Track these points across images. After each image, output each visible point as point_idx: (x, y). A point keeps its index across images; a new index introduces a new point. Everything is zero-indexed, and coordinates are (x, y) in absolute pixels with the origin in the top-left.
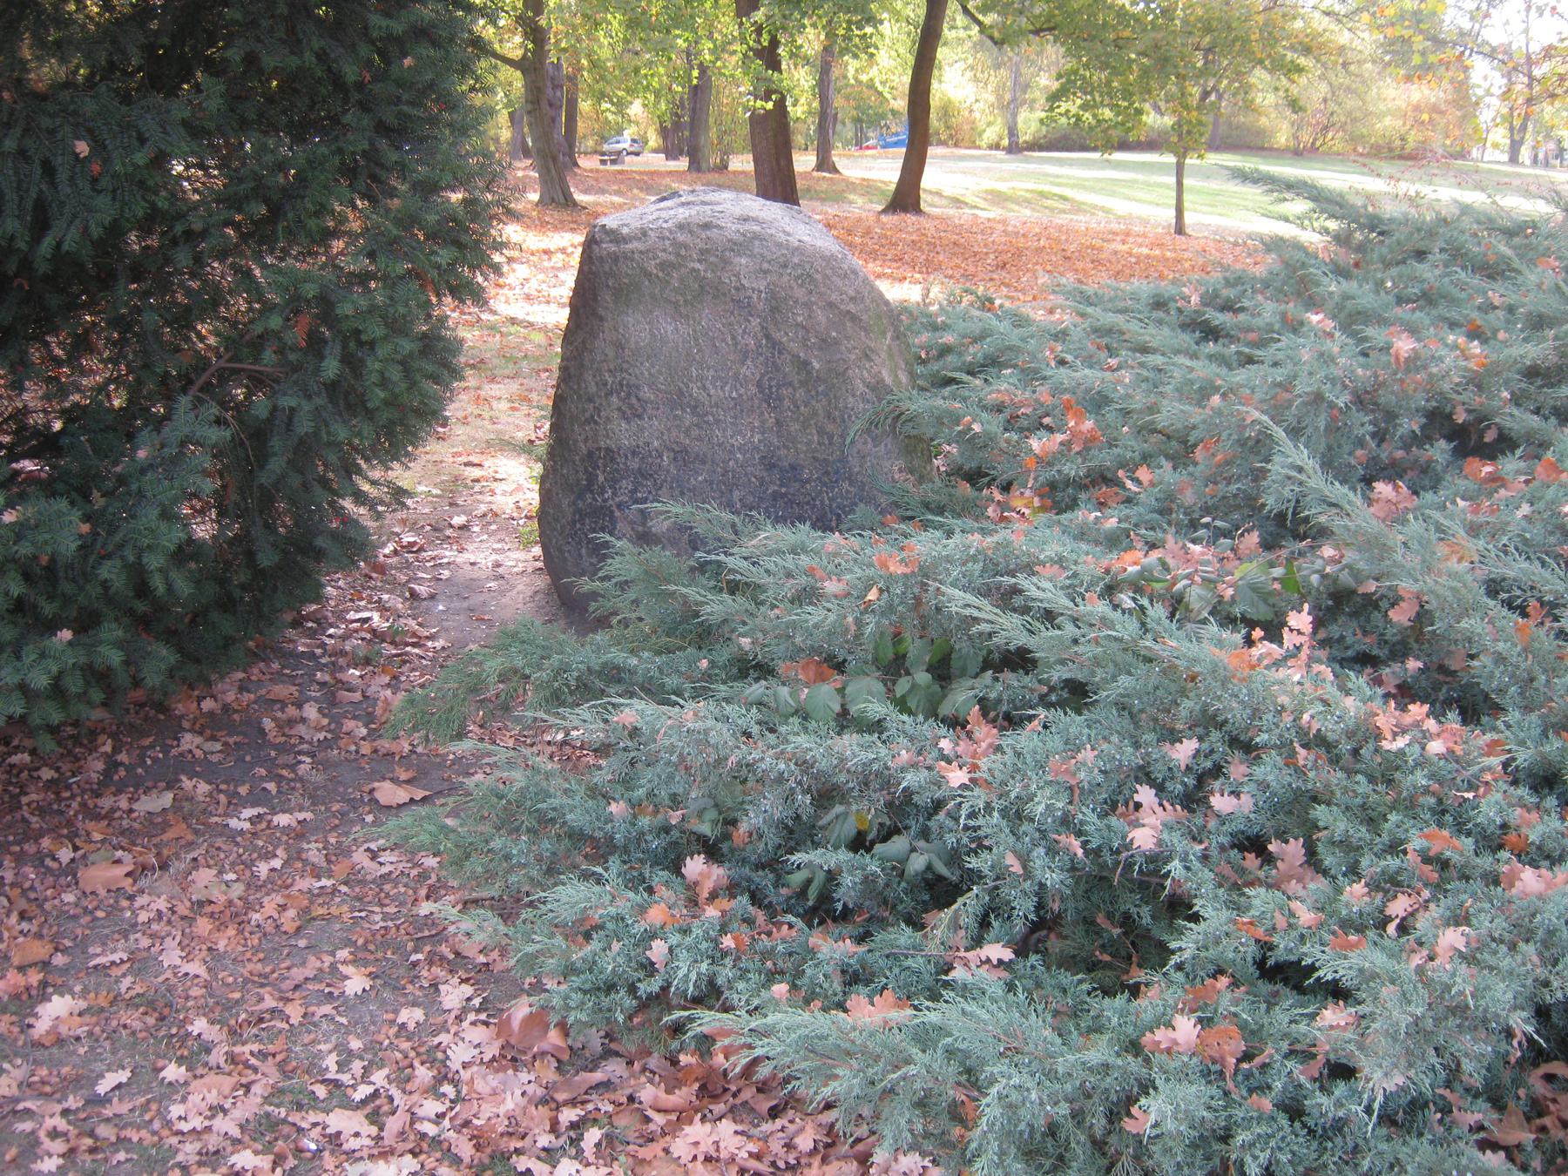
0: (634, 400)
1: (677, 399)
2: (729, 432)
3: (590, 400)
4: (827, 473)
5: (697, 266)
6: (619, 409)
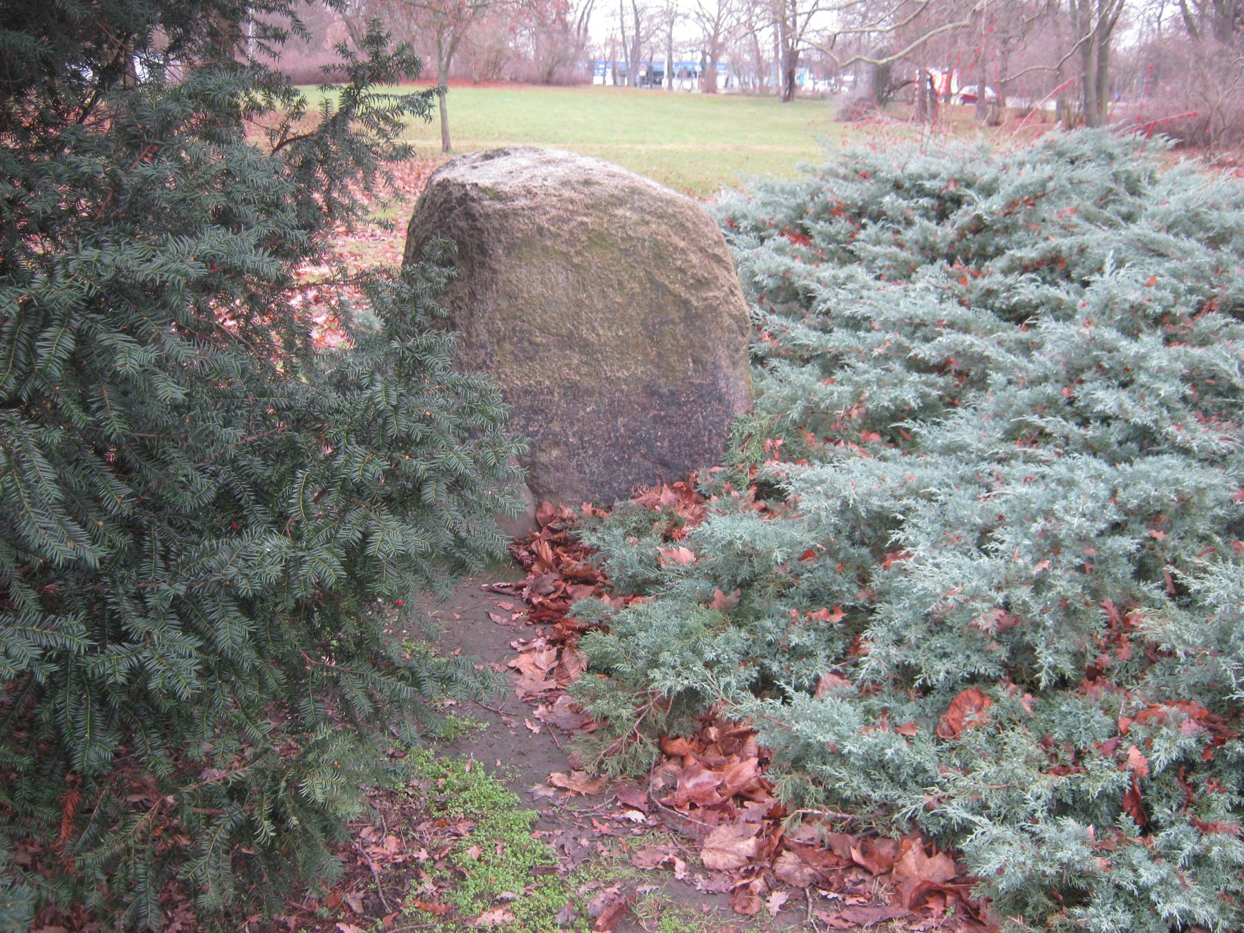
0: (526, 344)
1: (570, 341)
2: (616, 368)
3: (483, 347)
4: (701, 396)
5: (585, 219)
6: (512, 353)
